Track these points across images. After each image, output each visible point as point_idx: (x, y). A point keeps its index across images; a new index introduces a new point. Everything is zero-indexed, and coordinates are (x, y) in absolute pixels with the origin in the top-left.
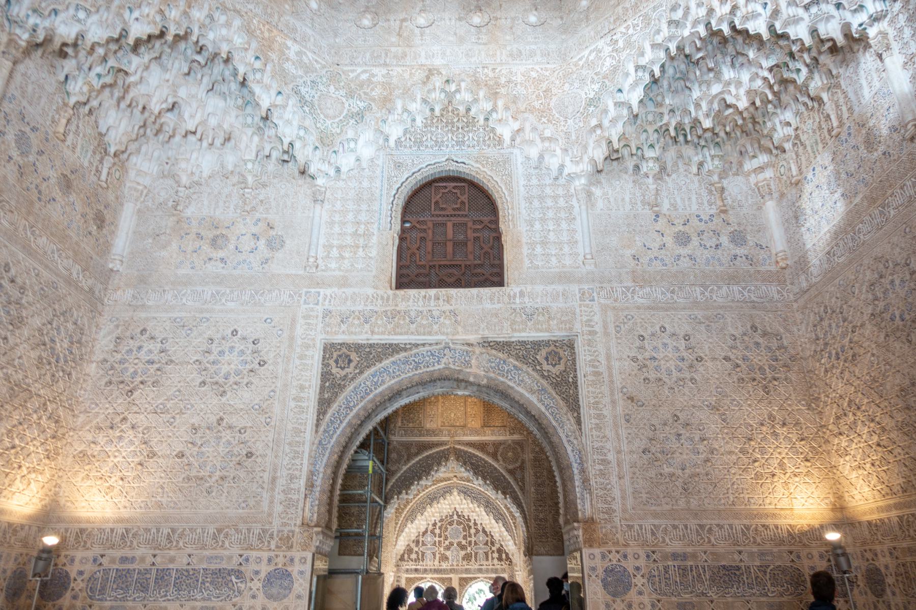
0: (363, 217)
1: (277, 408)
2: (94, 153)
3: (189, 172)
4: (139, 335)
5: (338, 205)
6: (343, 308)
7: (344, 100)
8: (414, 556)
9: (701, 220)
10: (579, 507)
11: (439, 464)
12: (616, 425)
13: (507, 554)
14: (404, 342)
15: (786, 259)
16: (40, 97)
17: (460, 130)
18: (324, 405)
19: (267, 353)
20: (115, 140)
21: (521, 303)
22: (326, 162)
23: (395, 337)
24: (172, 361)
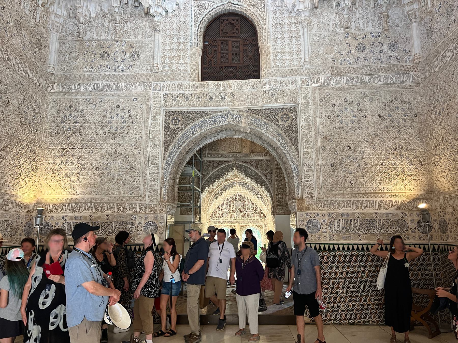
0: (182, 39)
1: (143, 145)
3: (84, 14)
4: (69, 108)
6: (174, 92)
8: (217, 215)
9: (373, 36)
10: (296, 192)
11: (228, 172)
12: (317, 152)
13: (264, 214)
14: (207, 110)
15: (419, 58)
18: (167, 144)
19: (136, 117)
24: (87, 122)
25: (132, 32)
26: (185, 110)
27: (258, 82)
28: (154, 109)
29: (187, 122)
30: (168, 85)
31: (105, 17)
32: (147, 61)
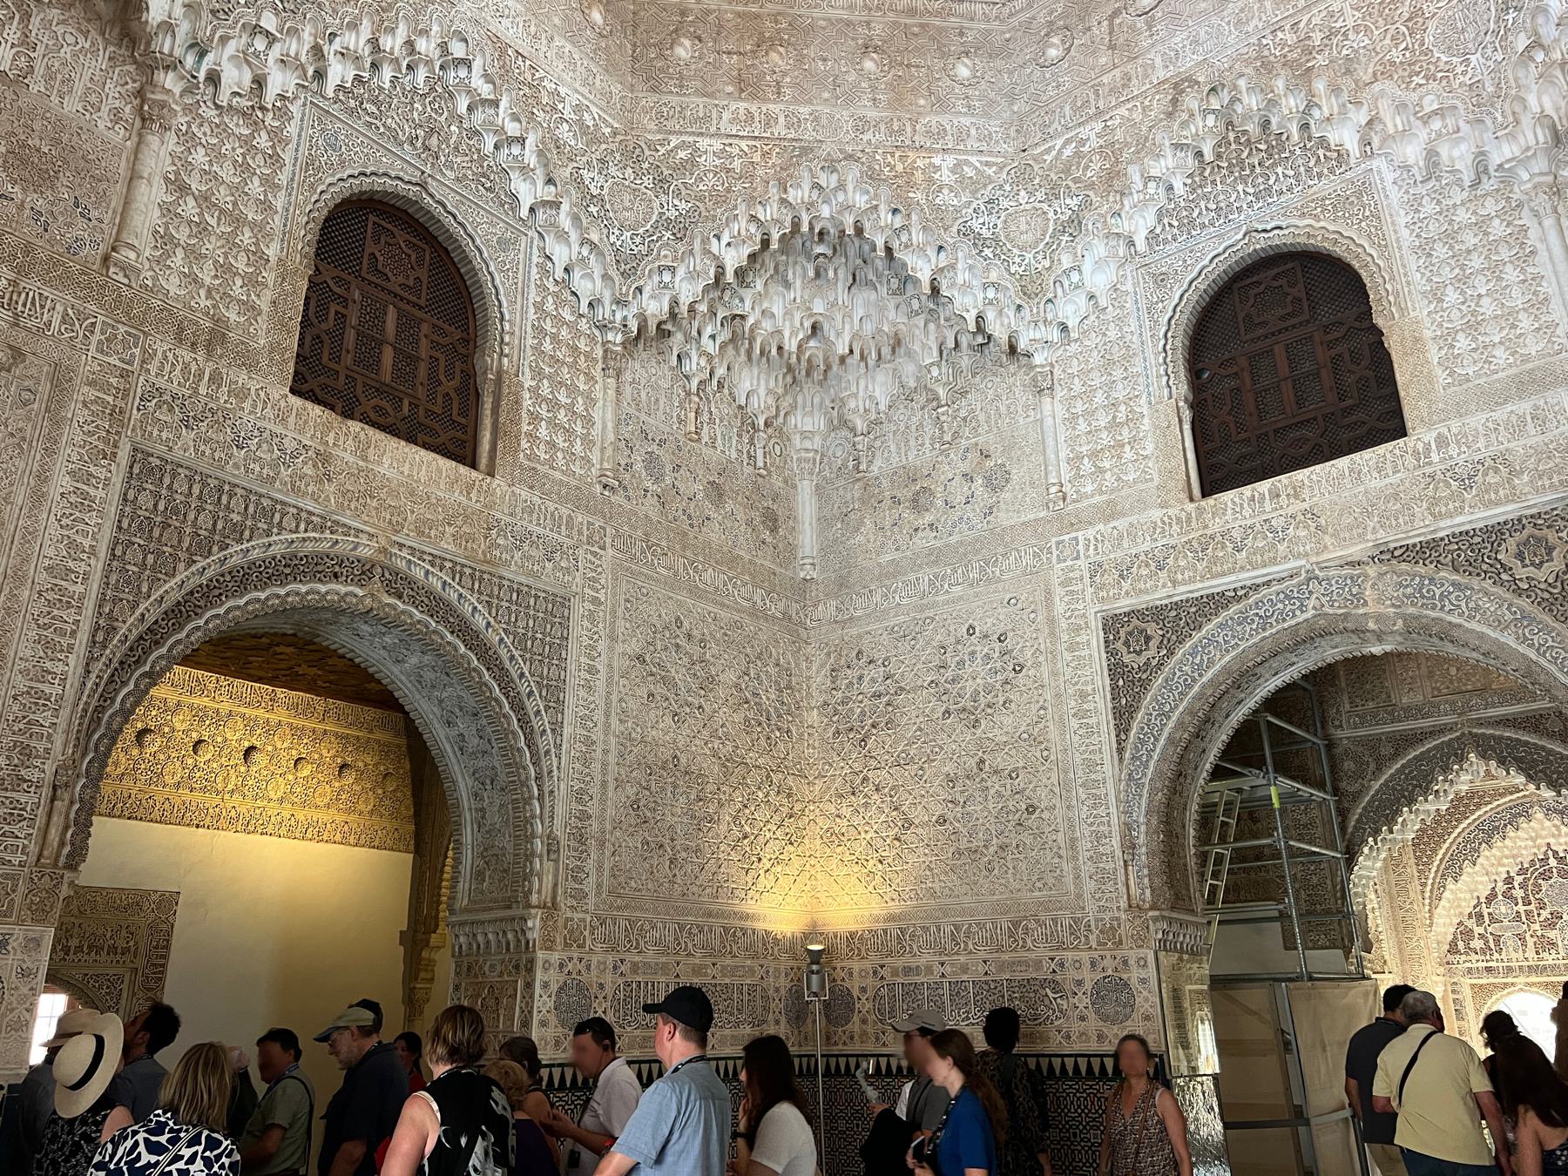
1: (1053, 733)
2: (739, 436)
3: (862, 411)
4: (855, 661)
5: (1077, 385)
6: (1119, 554)
7: (1045, 206)
8: (1477, 944)
11: (1446, 769)
14: (1232, 586)
16: (657, 400)
17: (1258, 170)
18: (1123, 717)
20: (761, 404)
21: (1442, 460)
22: (1041, 324)
23: (1214, 582)
24: (902, 689)
25: (982, 417)
26: (1160, 599)
27: (1397, 452)
28: (1070, 617)
29: (1174, 637)
30: (1099, 536)
31: (912, 400)
32: (1032, 484)
